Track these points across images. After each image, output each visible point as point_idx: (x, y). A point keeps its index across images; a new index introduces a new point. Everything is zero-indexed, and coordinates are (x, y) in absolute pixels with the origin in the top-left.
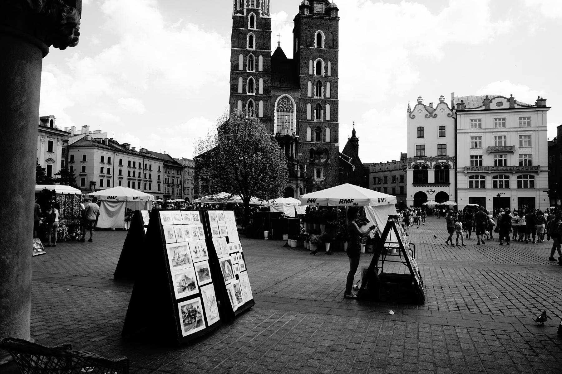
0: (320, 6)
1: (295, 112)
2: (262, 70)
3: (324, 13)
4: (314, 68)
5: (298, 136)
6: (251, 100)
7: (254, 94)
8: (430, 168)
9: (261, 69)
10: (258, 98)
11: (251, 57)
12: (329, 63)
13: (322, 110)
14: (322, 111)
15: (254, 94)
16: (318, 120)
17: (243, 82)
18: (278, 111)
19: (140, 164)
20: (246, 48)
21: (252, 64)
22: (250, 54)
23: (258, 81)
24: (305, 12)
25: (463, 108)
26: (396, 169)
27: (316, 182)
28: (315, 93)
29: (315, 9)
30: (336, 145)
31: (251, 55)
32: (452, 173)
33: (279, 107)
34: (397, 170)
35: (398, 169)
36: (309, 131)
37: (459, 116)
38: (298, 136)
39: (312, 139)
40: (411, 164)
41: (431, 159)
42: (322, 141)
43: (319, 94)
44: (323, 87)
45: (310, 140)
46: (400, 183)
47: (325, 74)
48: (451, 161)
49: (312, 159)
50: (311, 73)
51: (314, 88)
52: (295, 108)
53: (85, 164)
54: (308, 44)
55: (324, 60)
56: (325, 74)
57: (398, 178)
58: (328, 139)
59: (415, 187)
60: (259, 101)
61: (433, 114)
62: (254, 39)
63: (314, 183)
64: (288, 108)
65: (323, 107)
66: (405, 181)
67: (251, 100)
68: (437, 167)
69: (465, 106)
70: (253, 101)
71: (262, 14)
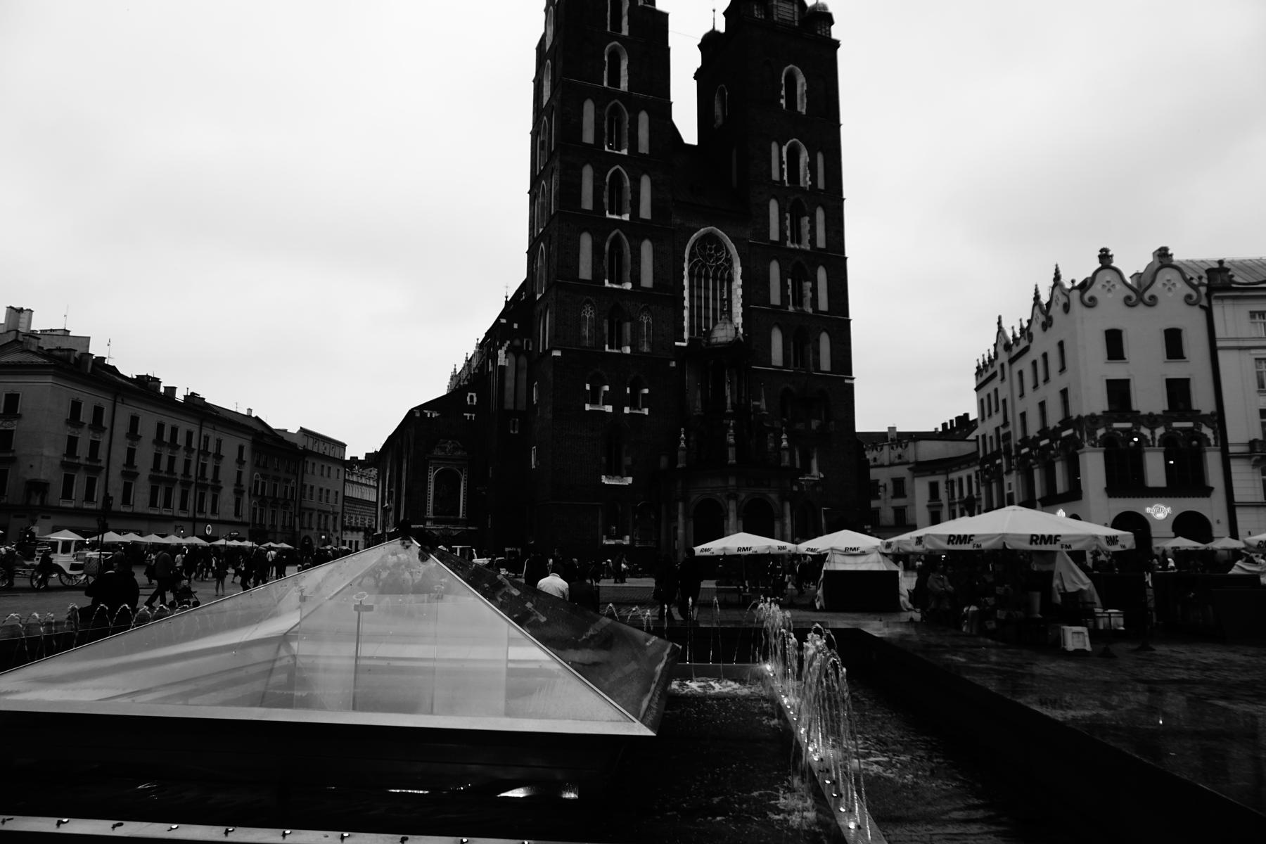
0: (787, 6)
1: (738, 281)
2: (647, 153)
3: (796, 24)
4: (784, 163)
7: (626, 217)
8: (1151, 443)
9: (644, 147)
10: (637, 230)
11: (615, 109)
12: (820, 157)
13: (806, 281)
14: (808, 285)
16: (798, 308)
17: (595, 179)
19: (190, 434)
20: (603, 84)
22: (612, 103)
24: (756, 12)
25: (1226, 279)
26: (878, 463)
29: (775, 10)
30: (847, 381)
32: (1213, 460)
33: (695, 264)
34: (882, 466)
35: (886, 463)
37: (1220, 302)
40: (1095, 433)
41: (1152, 420)
42: (812, 368)
43: (797, 238)
44: (807, 219)
45: (780, 364)
46: (893, 497)
47: (810, 183)
48: (1208, 426)
49: (785, 419)
50: (775, 175)
51: (786, 219)
52: (738, 270)
53: (13, 425)
56: (810, 183)
57: (885, 486)
58: (825, 364)
59: (1111, 499)
60: (643, 240)
61: (1146, 296)
62: (624, 64)
63: (795, 488)
64: (718, 268)
66: (907, 492)
67: (618, 234)
68: (1170, 445)
69: (1232, 276)
70: (624, 237)
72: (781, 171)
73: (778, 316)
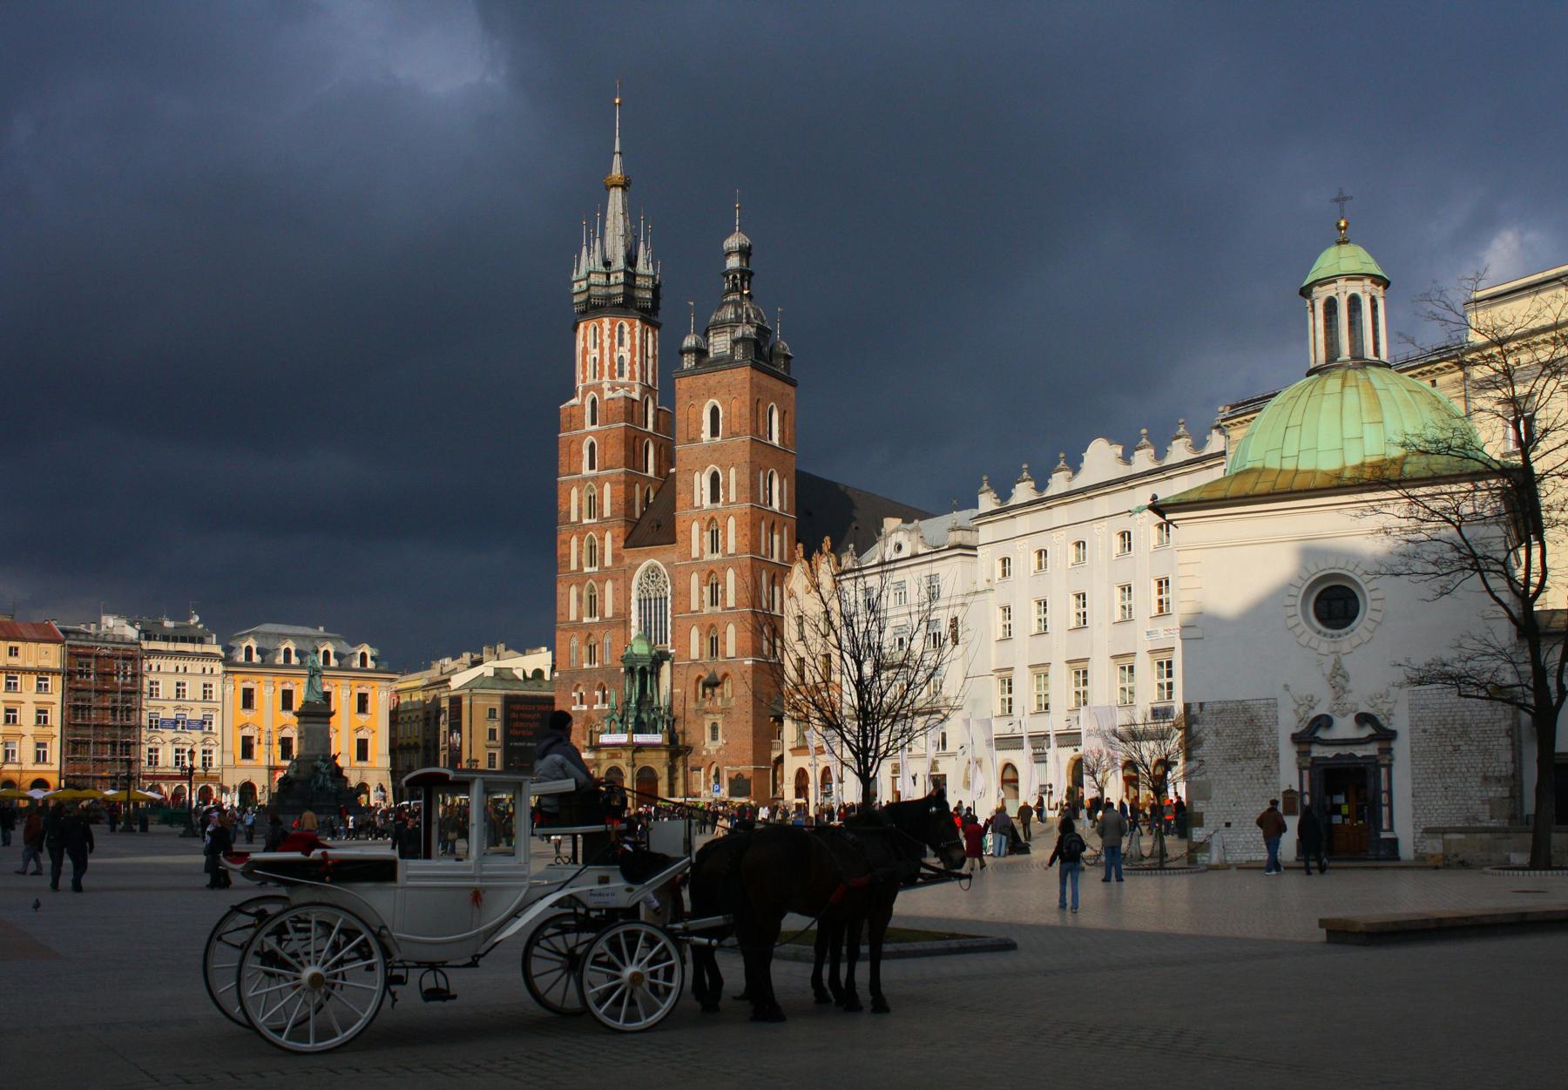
0: (723, 338)
1: (669, 598)
3: (729, 352)
4: (702, 489)
5: (673, 651)
6: (591, 584)
9: (607, 513)
11: (592, 490)
14: (720, 587)
15: (596, 569)
17: (578, 546)
18: (640, 601)
21: (594, 506)
23: (602, 539)
27: (709, 751)
28: (707, 548)
29: (711, 349)
30: (746, 663)
31: (590, 486)
36: (695, 633)
38: (673, 651)
39: (701, 655)
45: (697, 657)
50: (697, 504)
52: (669, 587)
54: (691, 437)
55: (721, 466)
58: (731, 652)
63: (704, 753)
65: (721, 580)
70: (594, 584)
71: (613, 389)
72: (702, 496)
73: (696, 616)
